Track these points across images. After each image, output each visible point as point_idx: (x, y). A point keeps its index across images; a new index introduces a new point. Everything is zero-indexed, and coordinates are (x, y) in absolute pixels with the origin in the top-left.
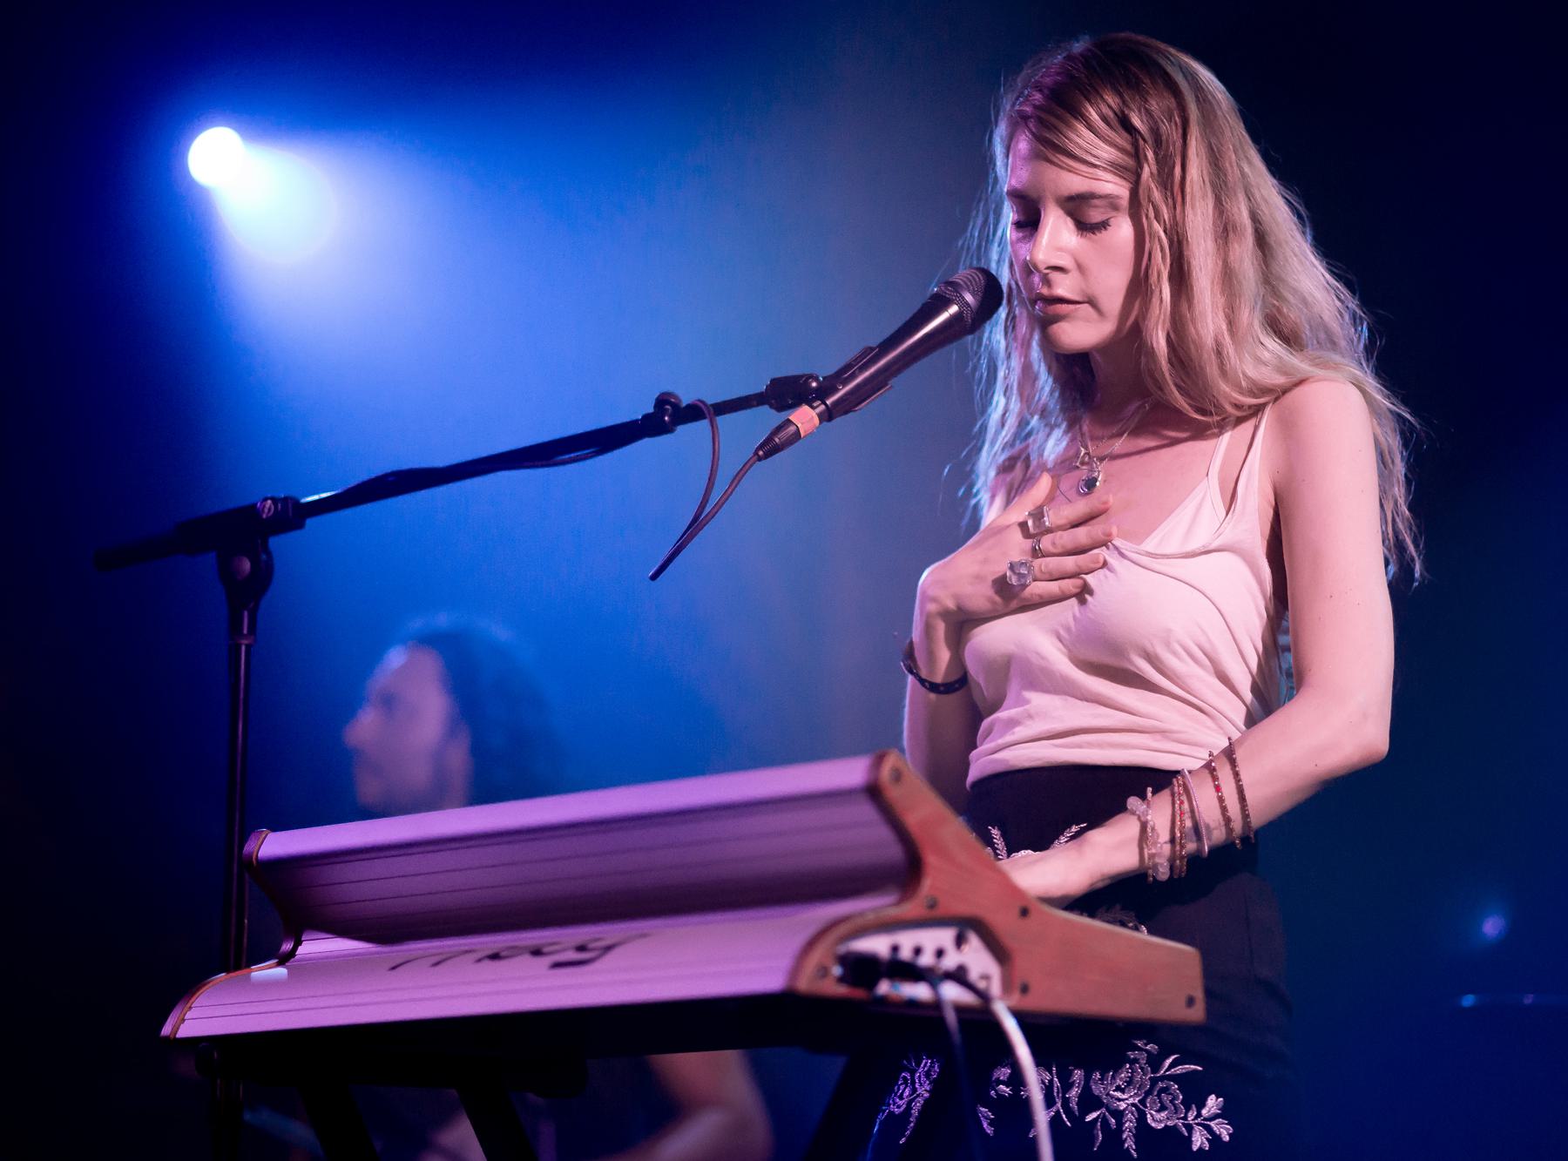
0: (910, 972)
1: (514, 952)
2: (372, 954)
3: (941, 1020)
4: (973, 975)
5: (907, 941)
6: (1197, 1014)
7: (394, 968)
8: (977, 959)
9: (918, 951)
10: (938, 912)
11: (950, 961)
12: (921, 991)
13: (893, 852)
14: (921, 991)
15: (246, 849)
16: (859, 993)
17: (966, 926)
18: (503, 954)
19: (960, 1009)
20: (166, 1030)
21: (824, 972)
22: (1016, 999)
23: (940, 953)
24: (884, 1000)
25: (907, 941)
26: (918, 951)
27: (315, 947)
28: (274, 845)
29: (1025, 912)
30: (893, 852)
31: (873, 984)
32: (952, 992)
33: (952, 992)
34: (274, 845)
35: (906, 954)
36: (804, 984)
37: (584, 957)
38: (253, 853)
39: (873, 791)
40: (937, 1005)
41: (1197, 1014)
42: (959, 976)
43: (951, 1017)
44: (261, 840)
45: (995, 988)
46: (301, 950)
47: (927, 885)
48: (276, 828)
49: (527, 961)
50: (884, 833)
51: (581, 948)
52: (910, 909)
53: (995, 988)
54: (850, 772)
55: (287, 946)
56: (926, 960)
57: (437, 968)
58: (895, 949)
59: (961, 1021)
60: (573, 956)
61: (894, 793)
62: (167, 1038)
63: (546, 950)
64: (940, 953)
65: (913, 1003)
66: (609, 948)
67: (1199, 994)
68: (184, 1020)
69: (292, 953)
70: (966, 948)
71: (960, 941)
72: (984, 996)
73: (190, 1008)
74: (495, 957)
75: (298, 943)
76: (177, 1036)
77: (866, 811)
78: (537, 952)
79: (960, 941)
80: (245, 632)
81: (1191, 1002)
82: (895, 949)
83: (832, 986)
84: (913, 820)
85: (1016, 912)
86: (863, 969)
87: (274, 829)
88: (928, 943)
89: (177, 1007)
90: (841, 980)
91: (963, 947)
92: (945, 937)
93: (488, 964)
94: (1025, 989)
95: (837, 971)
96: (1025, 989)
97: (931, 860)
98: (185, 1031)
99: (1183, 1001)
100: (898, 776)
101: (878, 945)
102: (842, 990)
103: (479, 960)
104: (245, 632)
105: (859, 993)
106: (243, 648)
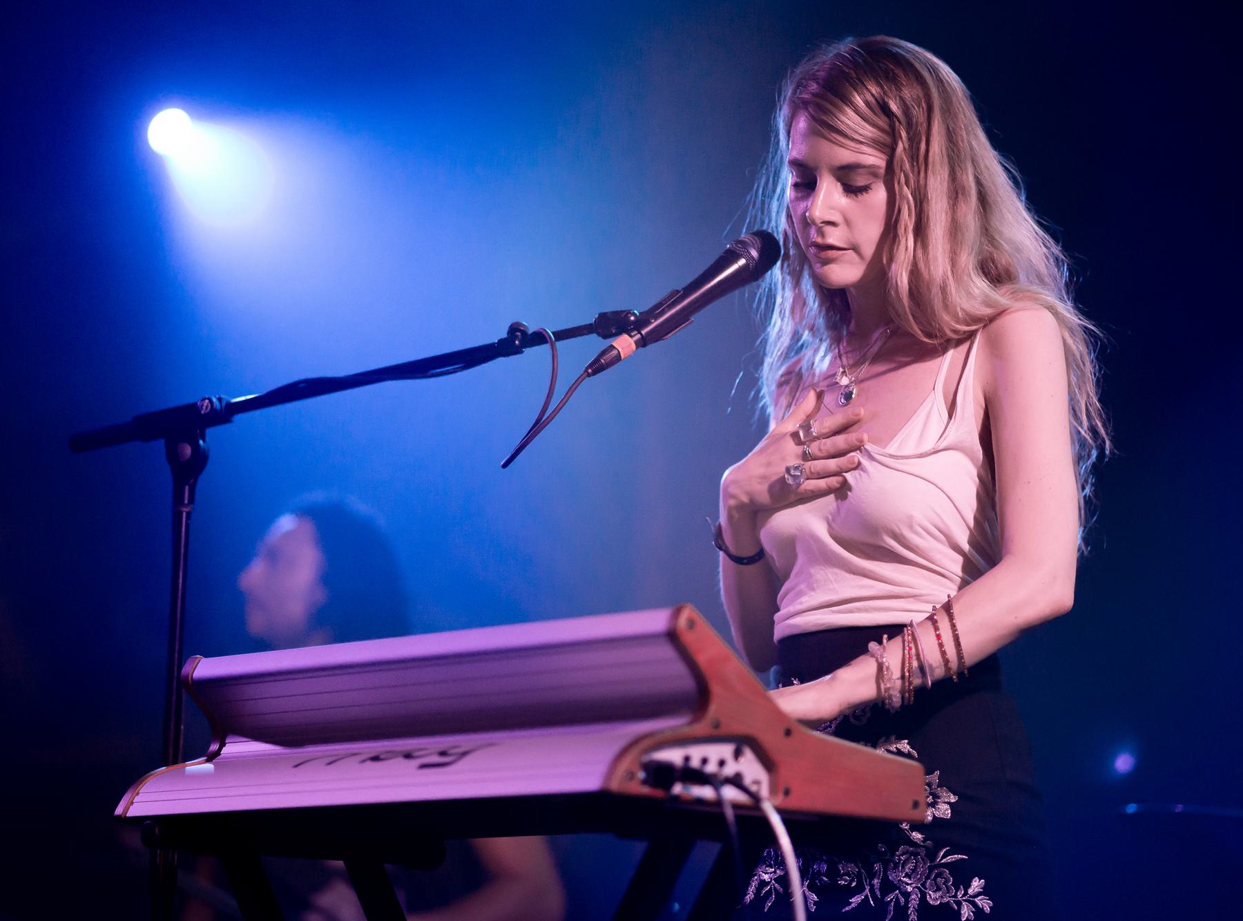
0: (698, 777)
1: (392, 755)
2: (280, 754)
3: (722, 816)
4: (747, 781)
5: (696, 753)
7: (296, 766)
8: (750, 768)
9: (705, 761)
10: (723, 731)
11: (730, 770)
12: (706, 792)
14: (706, 792)
15: (186, 669)
16: (659, 793)
17: (742, 742)
18: (382, 757)
19: (736, 806)
20: (119, 811)
21: (631, 775)
22: (780, 800)
23: (722, 763)
24: (677, 798)
25: (696, 753)
26: (705, 761)
27: (236, 748)
29: (788, 733)
31: (668, 786)
32: (730, 793)
33: (730, 793)
34: (206, 668)
35: (695, 763)
36: (615, 785)
37: (445, 759)
38: (188, 674)
39: (672, 636)
40: (719, 803)
42: (736, 781)
43: (729, 813)
45: (764, 791)
46: (225, 750)
47: (713, 709)
48: (208, 654)
50: (680, 668)
51: (443, 754)
52: (701, 728)
53: (764, 791)
55: (214, 747)
56: (711, 768)
57: (331, 765)
58: (687, 759)
59: (738, 817)
60: (436, 759)
61: (689, 638)
62: (119, 817)
64: (722, 763)
65: (700, 801)
66: (464, 754)
68: (132, 803)
69: (218, 753)
70: (742, 760)
71: (737, 754)
72: (756, 798)
73: (138, 794)
74: (376, 759)
75: (223, 745)
76: (129, 814)
77: (666, 651)
78: (408, 756)
79: (737, 754)
80: (186, 502)
82: (687, 759)
83: (638, 787)
84: (702, 659)
85: (782, 732)
86: (662, 774)
87: (206, 657)
88: (713, 755)
89: (128, 792)
91: (740, 759)
92: (726, 750)
93: (369, 763)
94: (787, 793)
95: (641, 775)
97: (716, 689)
98: (132, 812)
99: (910, 804)
100: (691, 624)
101: (674, 756)
102: (645, 790)
103: (364, 761)
104: (186, 502)
105: (659, 793)
106: (184, 514)
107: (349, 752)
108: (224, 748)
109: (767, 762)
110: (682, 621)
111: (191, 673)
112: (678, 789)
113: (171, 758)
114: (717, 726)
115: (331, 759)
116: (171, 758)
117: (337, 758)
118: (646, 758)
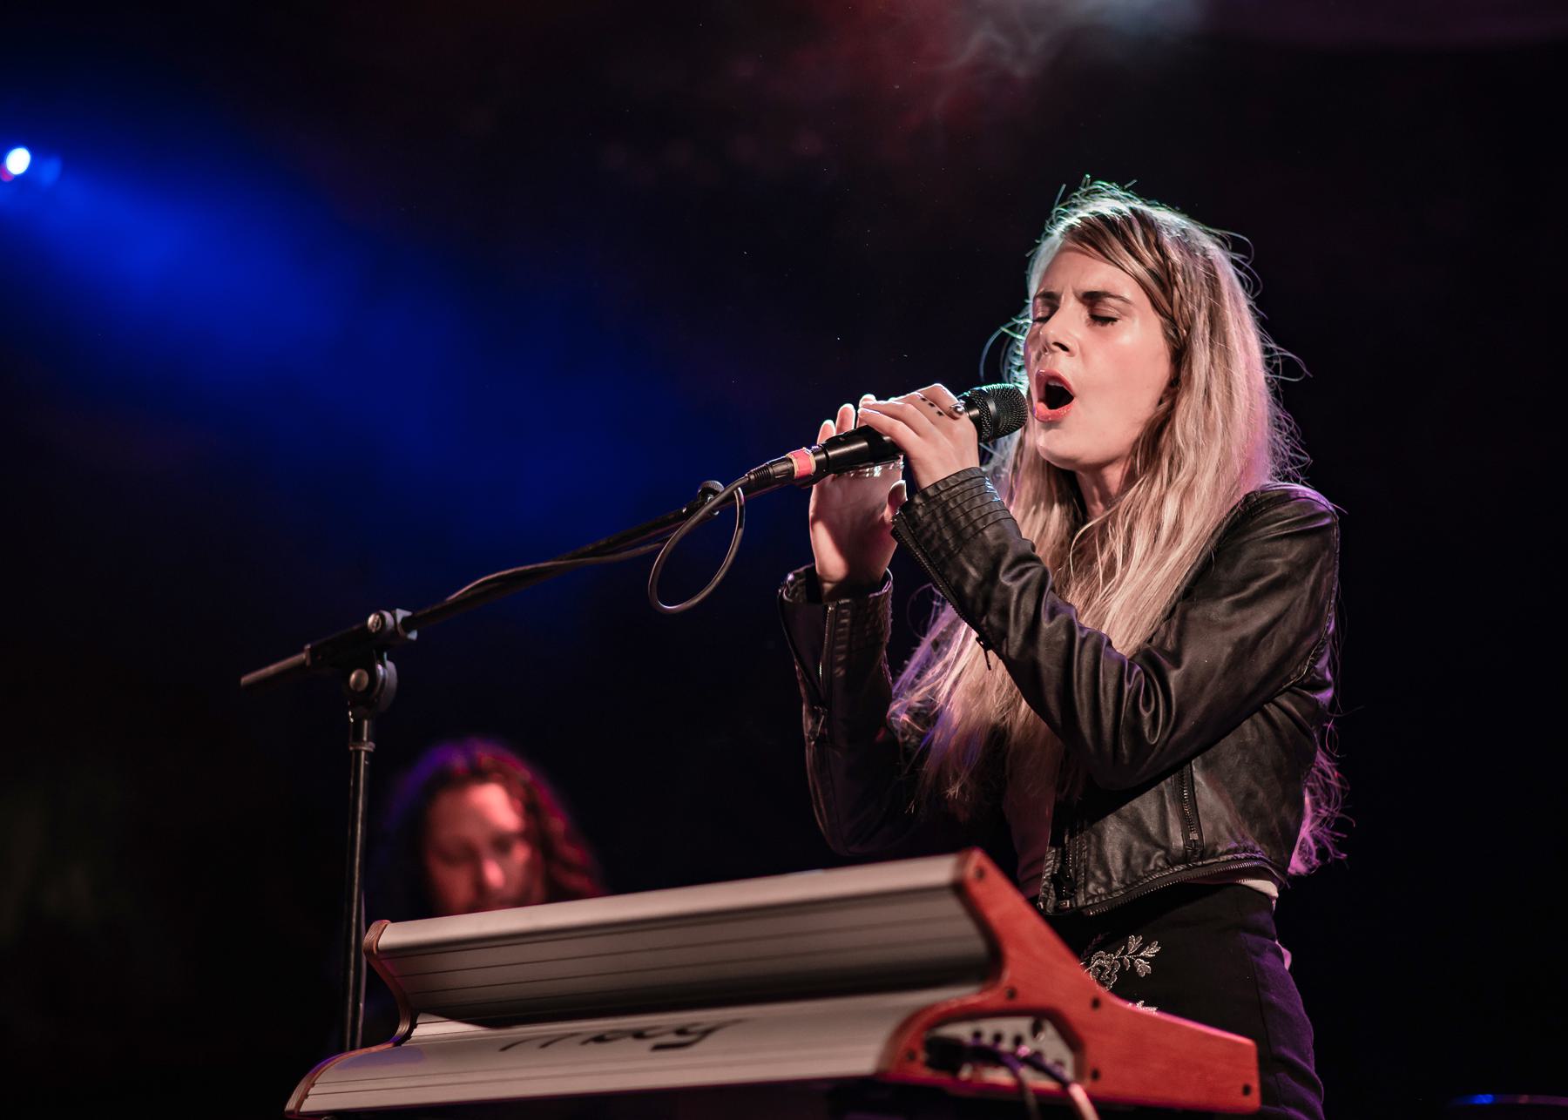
0: (990, 1056)
2: (482, 1036)
4: (1049, 1060)
6: (1253, 1101)
7: (504, 1049)
8: (1051, 1045)
9: (998, 1038)
10: (1019, 1002)
12: (1001, 1077)
13: (976, 945)
14: (1001, 1077)
15: (369, 938)
17: (1042, 1016)
18: (608, 1036)
19: (1040, 1093)
20: (291, 1105)
21: (912, 1056)
23: (1018, 1041)
25: (988, 1028)
26: (998, 1038)
27: (430, 1030)
28: (393, 934)
30: (977, 946)
31: (955, 1070)
34: (393, 934)
35: (987, 1040)
37: (685, 1039)
39: (958, 888)
40: (1020, 1086)
41: (1253, 1101)
42: (1035, 1062)
43: (1031, 1100)
44: (381, 929)
45: (1068, 1073)
46: (417, 1032)
47: (1007, 975)
49: (630, 1041)
50: (966, 927)
51: (681, 1032)
53: (1068, 1073)
54: (937, 871)
55: (403, 1028)
56: (1006, 1046)
57: (546, 1049)
58: (977, 1035)
61: (978, 890)
62: (291, 1112)
63: (648, 1033)
64: (1018, 1041)
65: (995, 1087)
66: (706, 1033)
67: (1255, 1085)
68: (306, 1096)
69: (408, 1035)
70: (1042, 1036)
71: (1036, 1030)
73: (313, 1085)
74: (600, 1039)
75: (413, 1026)
76: (303, 1109)
77: (952, 906)
78: (639, 1035)
80: (365, 739)
81: (1247, 1090)
82: (977, 1035)
84: (994, 914)
86: (948, 1054)
87: (393, 921)
88: (1012, 1027)
90: (929, 1064)
92: (1023, 1025)
93: (592, 1045)
94: (1096, 1075)
95: (922, 1056)
96: (1096, 1075)
97: (1012, 953)
98: (308, 1106)
99: (1239, 1090)
100: (981, 873)
101: (962, 1031)
102: (925, 1073)
103: (585, 1043)
105: (943, 1077)
106: (363, 754)
107: (569, 1032)
108: (415, 1030)
109: (1073, 1040)
110: (970, 871)
111: (375, 942)
112: (966, 1073)
113: (348, 1044)
114: (1012, 994)
115: (546, 1040)
116: (348, 1044)
117: (553, 1039)
118: (925, 1035)
